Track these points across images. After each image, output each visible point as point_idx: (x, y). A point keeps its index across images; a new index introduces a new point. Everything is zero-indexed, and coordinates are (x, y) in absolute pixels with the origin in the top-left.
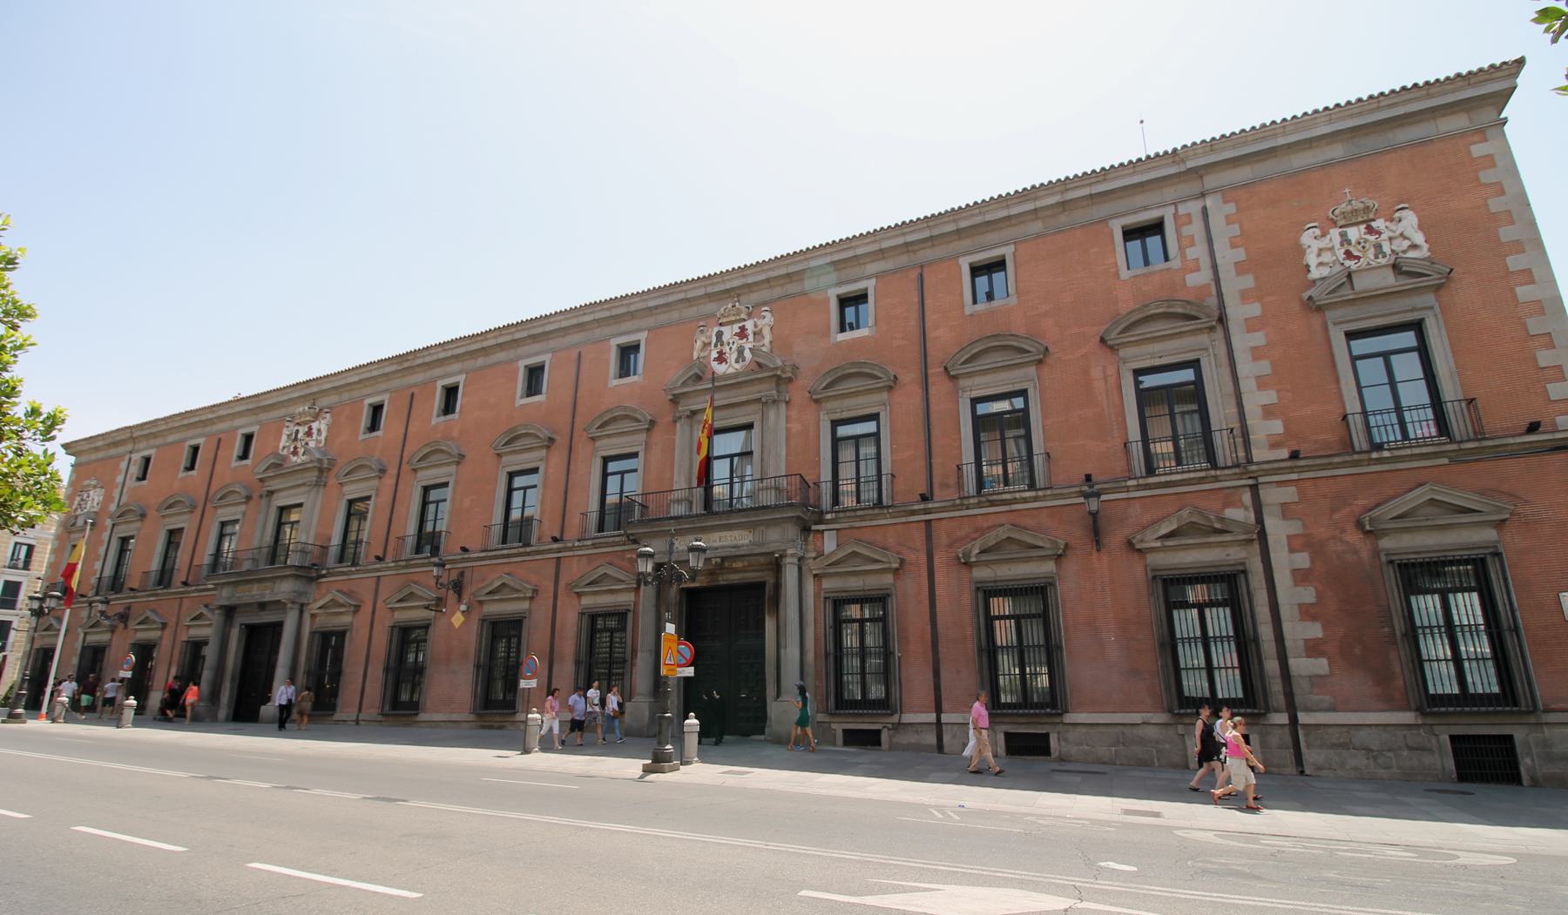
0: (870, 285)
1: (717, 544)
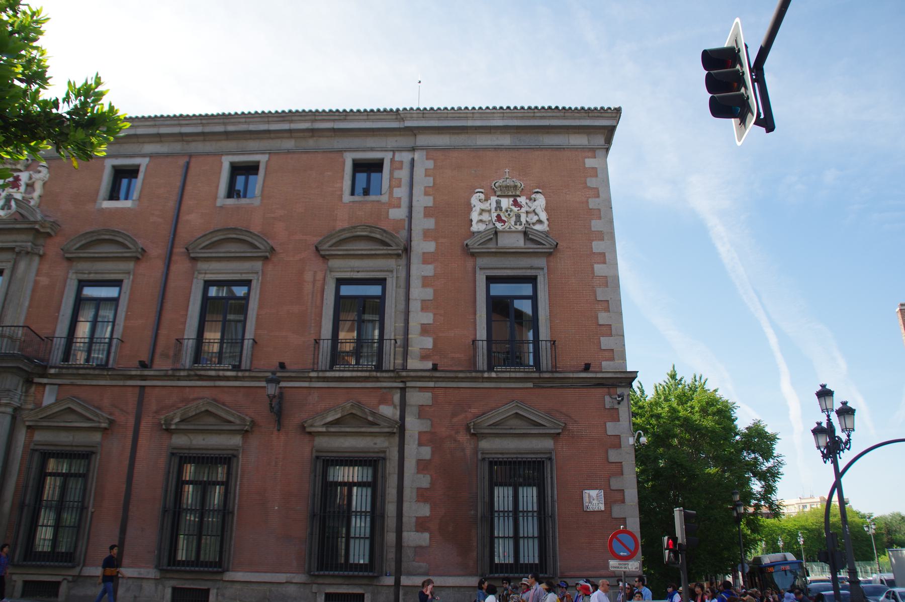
0: (143, 162)
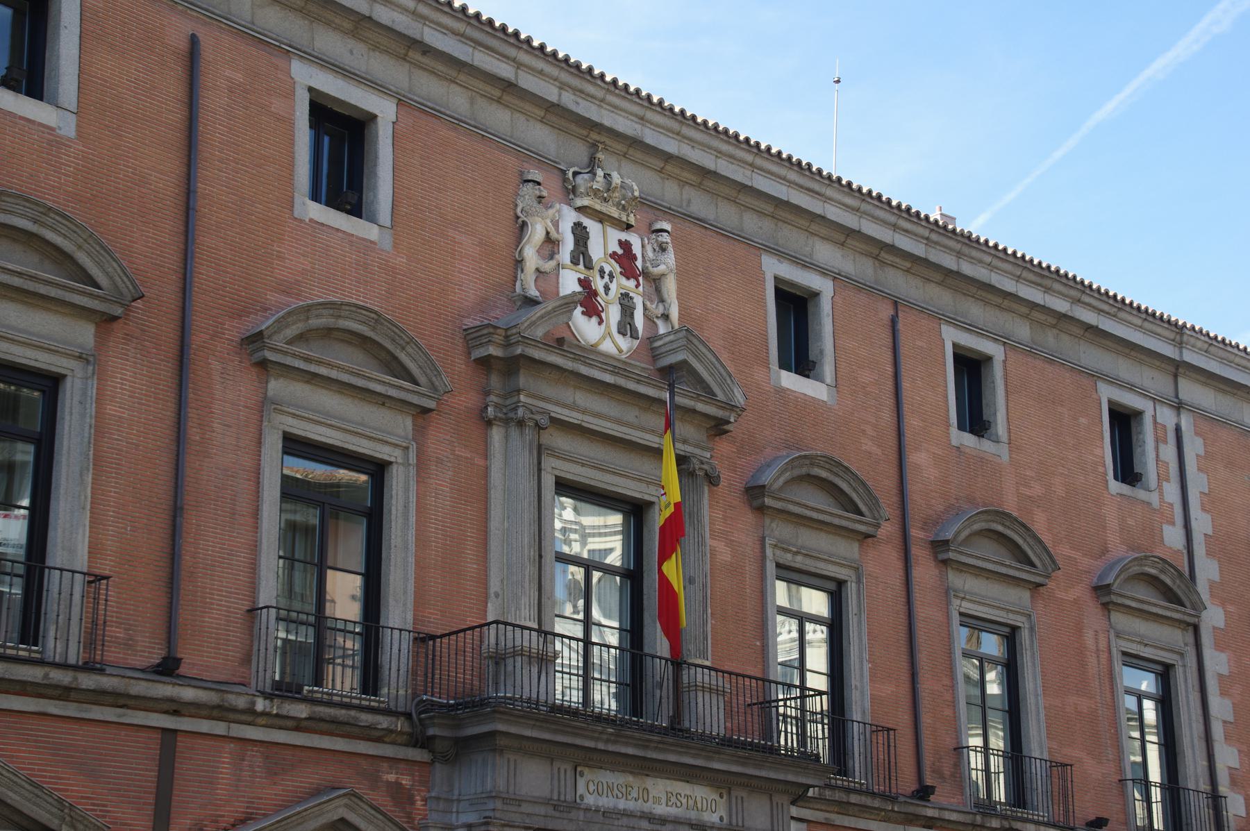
1: (661, 810)
